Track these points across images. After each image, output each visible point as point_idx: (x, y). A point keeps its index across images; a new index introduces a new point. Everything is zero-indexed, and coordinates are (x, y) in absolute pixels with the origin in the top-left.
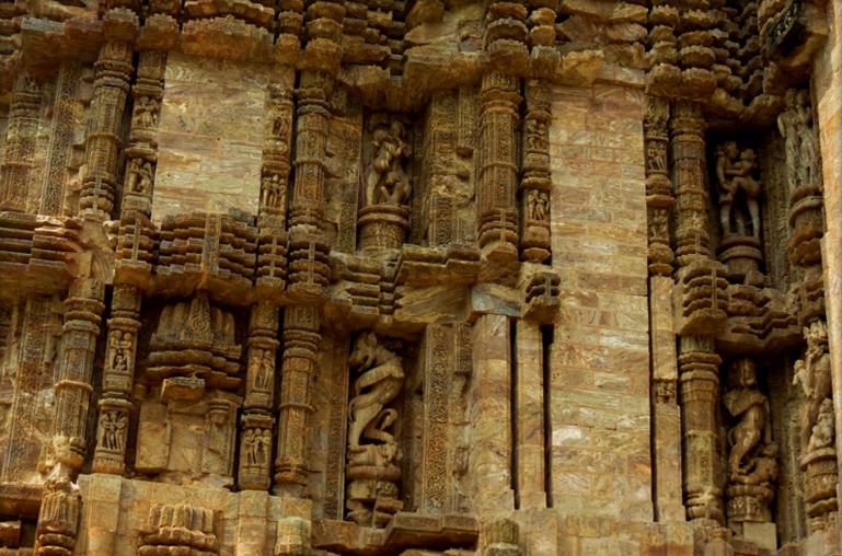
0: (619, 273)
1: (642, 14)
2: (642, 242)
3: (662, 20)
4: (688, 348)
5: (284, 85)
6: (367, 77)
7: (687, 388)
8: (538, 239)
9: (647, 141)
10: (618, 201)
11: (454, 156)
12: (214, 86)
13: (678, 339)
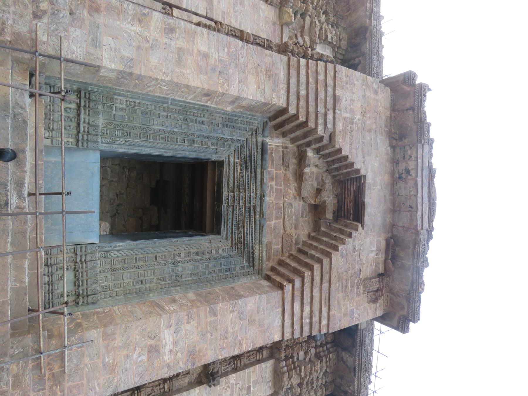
0: (214, 7)
1: (307, 45)
10: (241, 19)
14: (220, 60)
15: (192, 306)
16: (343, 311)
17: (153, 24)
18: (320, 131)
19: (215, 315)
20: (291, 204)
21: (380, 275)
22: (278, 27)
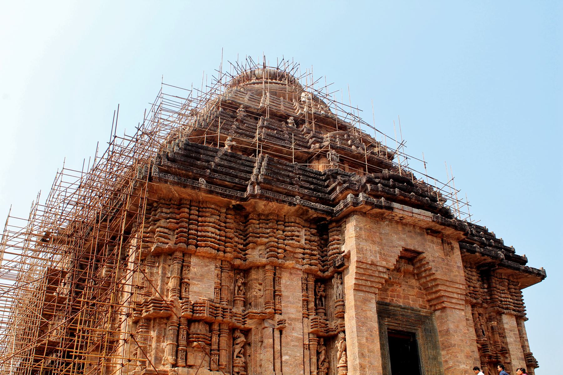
2: (301, 309)
3: (307, 254)
4: (311, 336)
5: (219, 264)
6: (237, 262)
7: (311, 346)
8: (279, 309)
9: (302, 283)
11: (258, 284)
12: (202, 264)
13: (309, 333)
14: (366, 331)
15: (451, 354)
16: (457, 273)
17: (363, 363)
18: (386, 276)
19: (455, 345)
20: (403, 290)
21: (442, 240)
22: (293, 271)
